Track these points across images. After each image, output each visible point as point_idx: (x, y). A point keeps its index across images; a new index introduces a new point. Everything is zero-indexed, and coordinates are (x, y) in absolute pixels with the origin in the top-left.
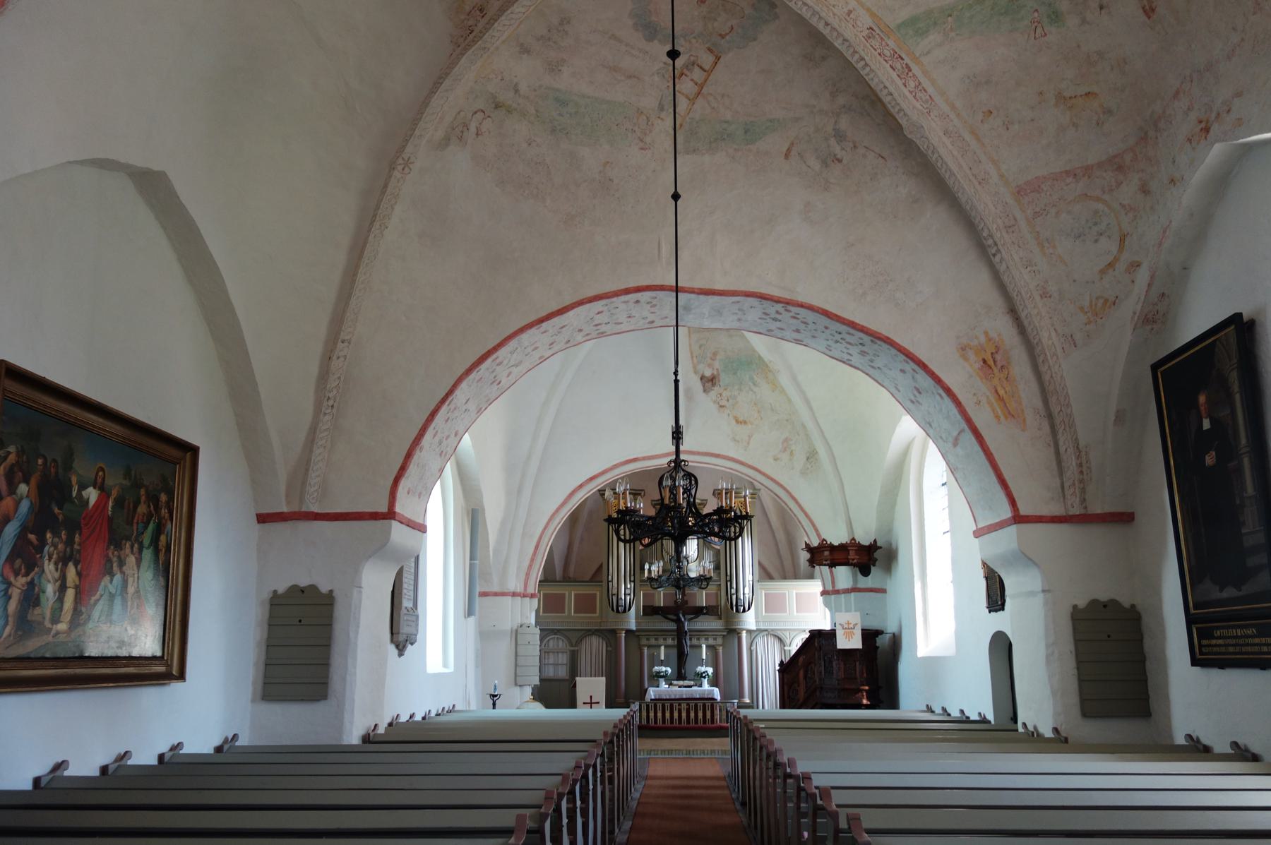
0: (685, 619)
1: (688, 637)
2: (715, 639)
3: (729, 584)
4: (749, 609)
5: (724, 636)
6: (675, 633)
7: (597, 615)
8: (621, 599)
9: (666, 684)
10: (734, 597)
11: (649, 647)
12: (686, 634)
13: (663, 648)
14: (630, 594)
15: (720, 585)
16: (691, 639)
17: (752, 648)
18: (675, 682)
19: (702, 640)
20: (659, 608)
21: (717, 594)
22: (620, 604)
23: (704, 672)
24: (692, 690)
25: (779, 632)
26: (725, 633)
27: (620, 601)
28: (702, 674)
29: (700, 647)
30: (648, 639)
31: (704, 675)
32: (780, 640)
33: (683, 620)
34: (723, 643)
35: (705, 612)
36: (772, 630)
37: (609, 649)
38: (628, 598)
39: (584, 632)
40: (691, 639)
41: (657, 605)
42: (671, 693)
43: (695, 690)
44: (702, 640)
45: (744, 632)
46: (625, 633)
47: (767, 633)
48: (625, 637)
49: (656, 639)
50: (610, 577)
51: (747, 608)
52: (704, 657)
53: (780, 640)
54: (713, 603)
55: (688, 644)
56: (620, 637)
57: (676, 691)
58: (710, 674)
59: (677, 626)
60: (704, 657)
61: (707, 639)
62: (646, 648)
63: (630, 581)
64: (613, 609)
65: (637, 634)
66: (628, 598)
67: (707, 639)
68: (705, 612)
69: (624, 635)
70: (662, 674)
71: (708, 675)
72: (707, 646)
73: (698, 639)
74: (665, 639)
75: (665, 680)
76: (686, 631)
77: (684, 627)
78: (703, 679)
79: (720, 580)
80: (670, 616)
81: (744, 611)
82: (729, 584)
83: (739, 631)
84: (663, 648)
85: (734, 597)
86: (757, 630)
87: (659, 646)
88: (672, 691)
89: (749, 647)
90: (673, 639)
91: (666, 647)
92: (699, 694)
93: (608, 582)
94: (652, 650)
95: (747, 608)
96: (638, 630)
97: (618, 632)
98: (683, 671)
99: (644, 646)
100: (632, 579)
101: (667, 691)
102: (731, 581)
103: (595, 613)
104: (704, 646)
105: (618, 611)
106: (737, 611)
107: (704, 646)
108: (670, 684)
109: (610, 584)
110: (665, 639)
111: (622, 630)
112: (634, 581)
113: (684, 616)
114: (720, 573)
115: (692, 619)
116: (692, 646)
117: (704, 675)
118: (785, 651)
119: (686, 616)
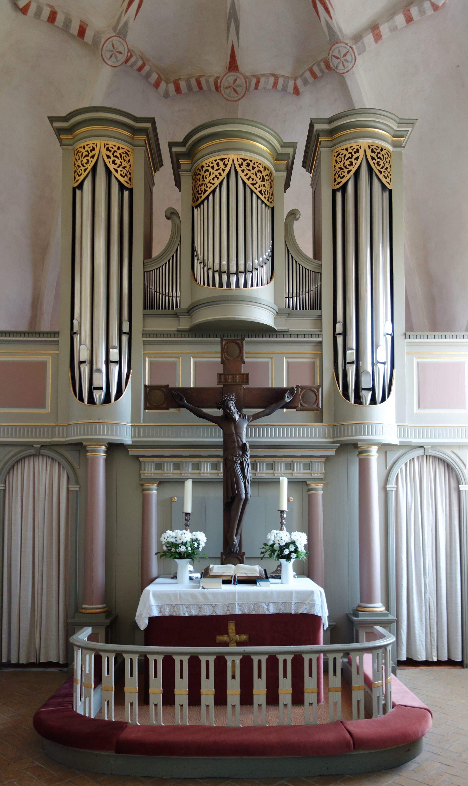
0: (242, 416)
1: (248, 460)
2: (308, 466)
3: (340, 340)
4: (383, 399)
5: (327, 458)
6: (220, 452)
7: (48, 410)
8: (99, 371)
9: (196, 571)
10: (352, 370)
11: (161, 483)
12: (244, 453)
13: (189, 484)
14: (119, 363)
15: (321, 343)
16: (254, 466)
17: (389, 487)
18: (216, 569)
19: (280, 468)
20: (185, 391)
21: (313, 364)
22: (95, 384)
23: (287, 546)
24: (257, 594)
25: (448, 452)
26: (332, 453)
27: (95, 375)
28: (282, 549)
29: (277, 483)
30: (159, 466)
31: (286, 552)
32: (448, 467)
33: (237, 417)
34: (325, 474)
35: (287, 400)
36: (434, 446)
37: (74, 488)
38: (115, 369)
39: (15, 450)
40: (254, 466)
41: (180, 383)
42: (201, 600)
43: (265, 594)
44: (280, 468)
45: (374, 449)
46: (106, 452)
47: (420, 452)
48: (108, 461)
49: (178, 466)
50: (75, 322)
51: (379, 396)
52: (285, 507)
53: (448, 467)
54: (305, 381)
55: (249, 472)
56: (94, 461)
57: (215, 595)
58: (301, 548)
59: (226, 436)
60: (285, 507)
61: (290, 466)
62: (155, 487)
63: (121, 332)
64: (81, 399)
65: (132, 452)
66: (115, 369)
67: (290, 466)
68: (287, 400)
69: (101, 456)
70: (183, 549)
71: (296, 551)
72: (290, 482)
73: (272, 466)
74: (197, 466)
75: (193, 563)
76: (243, 447)
77: (239, 435)
78: (283, 561)
79: (320, 335)
80: (205, 410)
81: (373, 401)
82: (340, 340)
83: (364, 448)
84: (189, 484)
85: (352, 370)
86: (403, 446)
87: (181, 482)
88: (204, 595)
89: (382, 484)
90: (215, 466)
91: (195, 483)
92: (276, 604)
93: (72, 334)
94: (169, 492)
95: (379, 396)
96: (134, 446)
97: (89, 448)
98: (236, 541)
99: (151, 480)
100: (126, 328)
101: (193, 596)
102: (344, 334)
103: (43, 406)
104: (284, 481)
105: (91, 401)
106: (358, 400)
107: (284, 481)
108: (206, 574)
109: (76, 338)
110: (197, 466)
111: (99, 442)
112: (130, 334)
113: (239, 409)
114: (320, 317)
115: (256, 417)
116: (257, 483)
117: (286, 552)
118: (459, 492)
119: (245, 411)
